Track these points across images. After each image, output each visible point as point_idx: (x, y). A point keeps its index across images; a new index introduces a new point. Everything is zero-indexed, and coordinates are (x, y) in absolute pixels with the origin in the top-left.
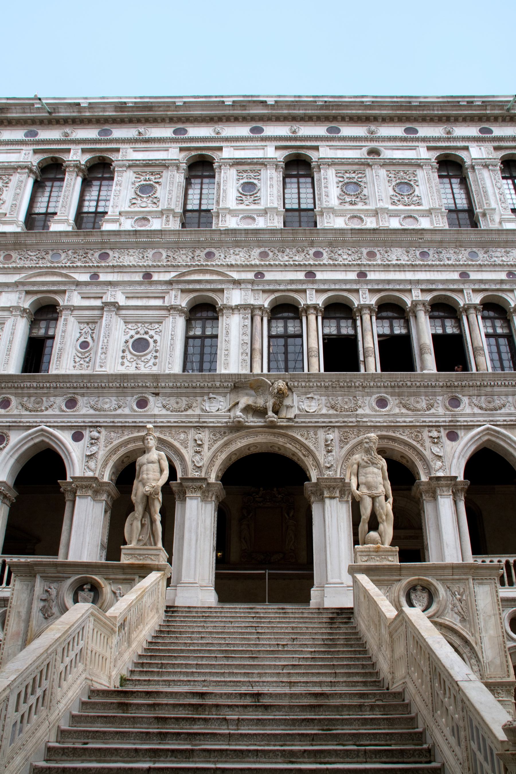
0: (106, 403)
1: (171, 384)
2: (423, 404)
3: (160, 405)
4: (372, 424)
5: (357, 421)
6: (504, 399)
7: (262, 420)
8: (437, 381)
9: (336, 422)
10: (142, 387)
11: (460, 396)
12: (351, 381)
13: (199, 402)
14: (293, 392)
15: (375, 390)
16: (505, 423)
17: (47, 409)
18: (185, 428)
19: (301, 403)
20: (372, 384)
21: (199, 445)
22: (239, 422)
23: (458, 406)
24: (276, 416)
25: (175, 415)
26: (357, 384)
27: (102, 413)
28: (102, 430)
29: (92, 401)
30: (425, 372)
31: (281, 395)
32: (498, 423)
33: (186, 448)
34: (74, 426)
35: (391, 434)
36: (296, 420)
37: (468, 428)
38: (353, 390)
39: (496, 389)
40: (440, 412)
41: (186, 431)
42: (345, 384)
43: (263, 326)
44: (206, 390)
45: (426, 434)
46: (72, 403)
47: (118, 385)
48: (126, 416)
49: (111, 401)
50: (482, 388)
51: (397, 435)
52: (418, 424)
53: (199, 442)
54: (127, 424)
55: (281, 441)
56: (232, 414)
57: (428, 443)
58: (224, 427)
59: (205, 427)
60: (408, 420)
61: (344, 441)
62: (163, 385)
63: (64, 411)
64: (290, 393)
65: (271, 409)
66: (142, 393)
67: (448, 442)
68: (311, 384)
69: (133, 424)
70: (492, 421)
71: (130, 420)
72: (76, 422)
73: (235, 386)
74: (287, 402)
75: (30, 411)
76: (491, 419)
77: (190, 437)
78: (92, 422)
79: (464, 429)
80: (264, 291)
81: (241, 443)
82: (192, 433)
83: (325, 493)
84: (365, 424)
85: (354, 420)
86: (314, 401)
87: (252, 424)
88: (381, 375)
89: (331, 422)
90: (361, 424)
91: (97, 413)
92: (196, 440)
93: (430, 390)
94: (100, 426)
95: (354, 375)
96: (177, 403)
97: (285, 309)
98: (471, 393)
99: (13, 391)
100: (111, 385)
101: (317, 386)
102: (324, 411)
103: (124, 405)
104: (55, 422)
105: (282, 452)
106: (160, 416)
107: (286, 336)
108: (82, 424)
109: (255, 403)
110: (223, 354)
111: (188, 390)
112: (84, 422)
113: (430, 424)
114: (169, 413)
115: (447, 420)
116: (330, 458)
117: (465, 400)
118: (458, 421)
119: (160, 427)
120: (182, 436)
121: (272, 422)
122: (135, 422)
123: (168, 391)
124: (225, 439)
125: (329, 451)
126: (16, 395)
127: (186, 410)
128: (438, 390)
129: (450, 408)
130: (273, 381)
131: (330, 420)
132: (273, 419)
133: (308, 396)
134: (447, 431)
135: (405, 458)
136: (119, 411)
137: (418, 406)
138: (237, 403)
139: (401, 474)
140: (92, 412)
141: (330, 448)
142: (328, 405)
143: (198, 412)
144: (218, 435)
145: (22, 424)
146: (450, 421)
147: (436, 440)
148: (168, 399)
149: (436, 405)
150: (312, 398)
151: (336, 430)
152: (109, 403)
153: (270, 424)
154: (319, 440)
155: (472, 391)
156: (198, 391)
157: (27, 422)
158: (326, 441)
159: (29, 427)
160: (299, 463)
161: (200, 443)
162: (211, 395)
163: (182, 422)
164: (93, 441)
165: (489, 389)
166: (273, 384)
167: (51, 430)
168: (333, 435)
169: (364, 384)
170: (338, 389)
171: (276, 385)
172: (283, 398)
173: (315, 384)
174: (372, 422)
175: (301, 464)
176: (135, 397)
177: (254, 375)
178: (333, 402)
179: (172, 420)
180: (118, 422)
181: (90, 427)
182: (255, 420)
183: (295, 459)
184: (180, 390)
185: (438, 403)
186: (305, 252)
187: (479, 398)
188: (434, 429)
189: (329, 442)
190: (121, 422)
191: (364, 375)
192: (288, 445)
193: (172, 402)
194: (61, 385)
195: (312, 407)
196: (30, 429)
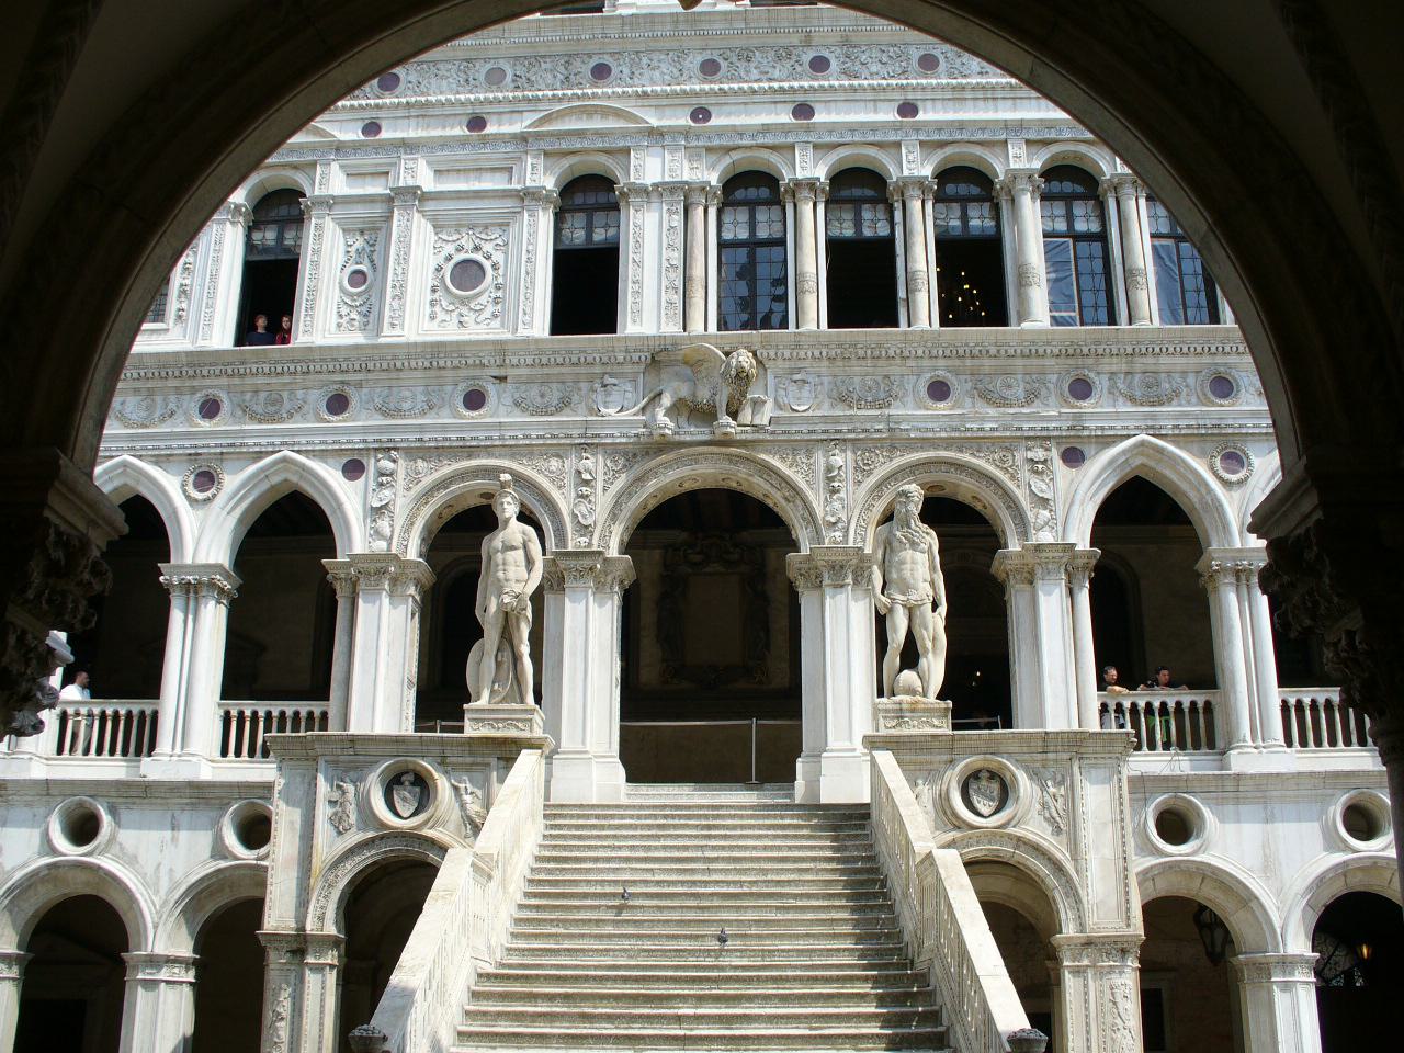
0: (405, 399)
3: (509, 401)
4: (919, 435)
5: (890, 430)
6: (1179, 380)
7: (706, 430)
8: (1048, 343)
10: (475, 366)
11: (1092, 375)
13: (584, 391)
14: (766, 370)
15: (926, 363)
16: (1177, 432)
17: (291, 416)
21: (587, 483)
24: (733, 423)
30: (1025, 325)
32: (1163, 432)
33: (560, 487)
34: (346, 450)
37: (1106, 441)
38: (880, 363)
39: (1164, 360)
41: (561, 453)
42: (869, 352)
43: (706, 227)
47: (427, 364)
49: (414, 397)
50: (1138, 359)
51: (966, 457)
53: (586, 476)
59: (597, 445)
60: (988, 426)
62: (515, 361)
65: (724, 408)
66: (474, 378)
68: (802, 354)
69: (461, 444)
70: (1152, 427)
73: (653, 358)
79: (1096, 443)
80: (709, 150)
84: (904, 435)
86: (807, 387)
87: (688, 438)
88: (939, 334)
89: (840, 431)
92: (580, 472)
93: (1035, 361)
94: (395, 449)
95: (887, 333)
96: (542, 396)
97: (751, 187)
98: (1114, 368)
99: (224, 381)
100: (413, 364)
102: (825, 411)
104: (308, 443)
107: (753, 244)
108: (361, 446)
109: (694, 395)
110: (630, 290)
113: (1032, 434)
117: (1101, 383)
118: (1084, 428)
120: (554, 463)
123: (524, 371)
125: (834, 491)
127: (559, 410)
130: (727, 348)
132: (729, 430)
134: (1063, 448)
135: (980, 501)
138: (660, 394)
141: (836, 484)
142: (835, 394)
146: (1069, 429)
147: (1040, 466)
148: (523, 387)
149: (1044, 392)
150: (804, 381)
153: (722, 438)
156: (583, 370)
160: (776, 510)
161: (588, 477)
162: (608, 380)
165: (1150, 360)
166: (727, 354)
169: (906, 353)
170: (854, 362)
172: (747, 385)
173: (810, 354)
174: (919, 430)
177: (690, 337)
178: (843, 389)
181: (376, 449)
184: (546, 370)
185: (1047, 388)
186: (794, 58)
187: (1130, 376)
191: (905, 333)
194: (318, 368)
196: (260, 458)
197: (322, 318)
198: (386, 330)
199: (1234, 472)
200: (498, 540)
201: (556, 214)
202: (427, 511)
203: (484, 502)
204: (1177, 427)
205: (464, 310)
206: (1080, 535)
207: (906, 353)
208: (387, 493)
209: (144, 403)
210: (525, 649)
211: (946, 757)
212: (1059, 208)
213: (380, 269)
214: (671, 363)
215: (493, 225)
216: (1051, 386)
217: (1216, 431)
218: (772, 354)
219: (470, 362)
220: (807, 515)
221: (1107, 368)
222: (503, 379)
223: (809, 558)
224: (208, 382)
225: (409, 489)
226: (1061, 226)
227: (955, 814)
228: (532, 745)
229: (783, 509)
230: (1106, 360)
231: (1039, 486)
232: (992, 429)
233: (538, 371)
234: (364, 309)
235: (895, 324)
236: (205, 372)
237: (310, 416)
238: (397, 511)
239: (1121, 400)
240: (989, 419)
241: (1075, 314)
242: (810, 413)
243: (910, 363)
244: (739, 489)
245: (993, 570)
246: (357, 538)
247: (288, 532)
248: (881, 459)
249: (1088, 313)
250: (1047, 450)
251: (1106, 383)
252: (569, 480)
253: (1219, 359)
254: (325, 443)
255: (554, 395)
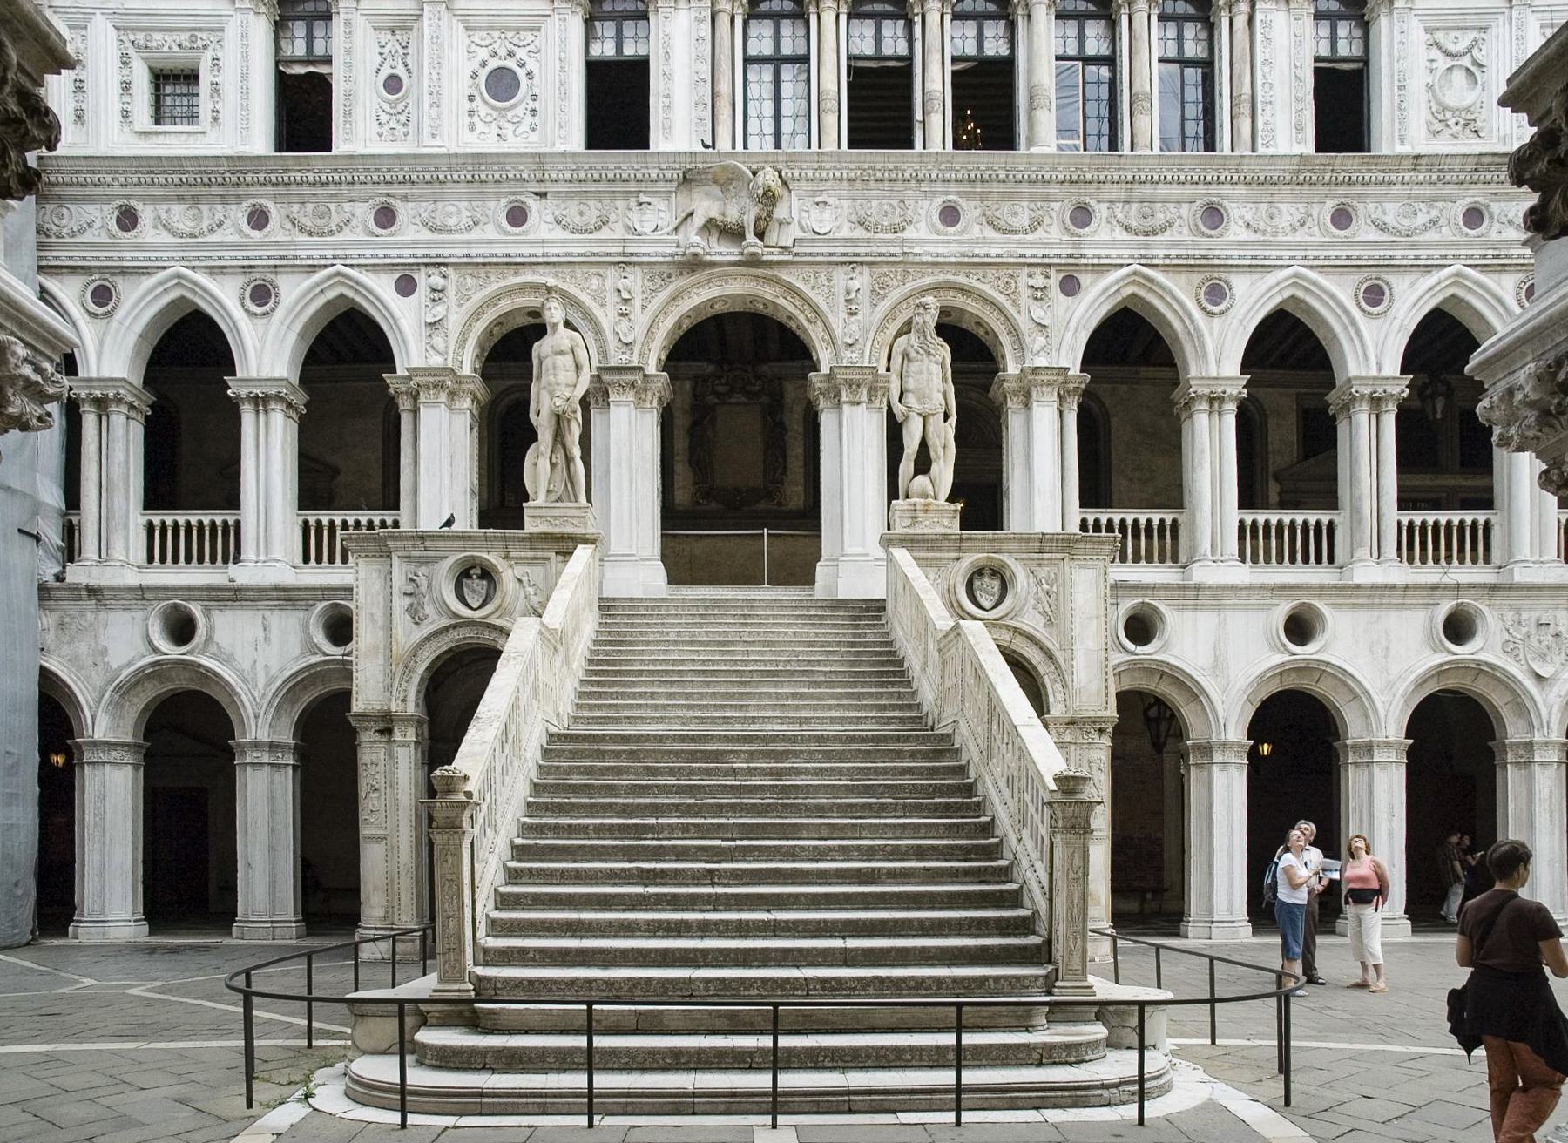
0: (450, 215)
1: (568, 176)
2: (1023, 220)
3: (550, 218)
4: (930, 259)
7: (736, 251)
9: (867, 254)
12: (897, 168)
15: (939, 187)
16: (1167, 261)
18: (597, 265)
19: (805, 214)
20: (934, 176)
22: (695, 255)
23: (1085, 224)
25: (579, 241)
26: (907, 176)
27: (445, 237)
28: (450, 271)
29: (425, 209)
31: (769, 199)
32: (1155, 261)
35: (961, 279)
36: (795, 250)
37: (1100, 268)
40: (1053, 238)
44: (633, 187)
45: (1023, 279)
46: (386, 217)
48: (490, 241)
50: (1136, 186)
52: (1012, 260)
54: (494, 260)
55: (768, 292)
56: (680, 237)
57: (1025, 293)
58: (668, 263)
59: (634, 264)
60: (993, 251)
61: (878, 293)
62: (554, 176)
63: (373, 234)
64: (786, 193)
66: (514, 193)
67: (1061, 296)
68: (824, 175)
70: (1145, 257)
71: (499, 251)
72: (399, 257)
74: (780, 212)
75: (310, 234)
76: (1143, 252)
77: (608, 283)
78: (428, 256)
81: (702, 295)
82: (612, 277)
83: (844, 394)
84: (917, 259)
85: (897, 250)
88: (953, 156)
89: (857, 255)
90: (911, 258)
91: (436, 236)
93: (1040, 188)
96: (581, 214)
98: (1114, 196)
101: (835, 179)
102: (845, 232)
103: (483, 219)
105: (769, 312)
106: (553, 241)
111: (601, 187)
112: (415, 256)
114: (567, 235)
115: (1064, 252)
116: (854, 327)
117: (1101, 211)
118: (1082, 256)
119: (554, 264)
120: (595, 282)
121: (753, 254)
122: (508, 255)
123: (562, 187)
124: (672, 287)
125: (852, 314)
126: (275, 199)
127: (598, 228)
128: (1054, 189)
129: (1072, 227)
130: (754, 167)
131: (857, 250)
133: (818, 199)
136: (475, 234)
137: (1015, 222)
139: (972, 353)
140: (426, 235)
142: (854, 218)
143: (619, 233)
144: (658, 280)
145: (298, 262)
149: (1047, 220)
151: (866, 269)
152: (456, 212)
154: (836, 290)
155: (1118, 192)
156: (619, 187)
157: (308, 258)
158: (848, 293)
159: (313, 268)
163: (594, 254)
164: (436, 295)
166: (754, 174)
167: (354, 273)
168: (861, 281)
169: (921, 176)
171: (760, 178)
172: (774, 205)
174: (930, 254)
175: (802, 336)
176: (504, 201)
179: (576, 251)
180: (478, 255)
181: (426, 265)
182: (723, 249)
183: (793, 325)
184: (584, 187)
188: (1039, 270)
189: (853, 296)
190: (483, 256)
191: (921, 155)
192: (781, 301)
193: (571, 210)
195: (822, 220)
197: (358, 127)
198: (428, 141)
199: (1216, 304)
200: (541, 348)
201: (586, 21)
202: (480, 327)
203: (532, 321)
204: (1167, 257)
205: (503, 123)
206: (1070, 356)
207: (921, 176)
208: (439, 311)
209: (191, 212)
210: (576, 452)
211: (954, 555)
212: (1072, 28)
213: (414, 74)
214: (702, 182)
215: (525, 29)
216: (1053, 214)
217: (1203, 262)
218: (796, 175)
219: (511, 176)
220: (827, 337)
221: (1106, 196)
222: (543, 195)
223: (830, 377)
224: (252, 190)
225: (460, 305)
226: (1072, 50)
227: (960, 606)
228: (585, 540)
229: (805, 331)
230: (1107, 187)
231: (1039, 313)
232: (998, 256)
233: (576, 187)
234: (403, 118)
235: (910, 145)
236: (248, 179)
237: (359, 230)
238: (450, 327)
239: (1118, 229)
240: (997, 246)
241: (1080, 142)
242: (831, 236)
243: (925, 187)
244: (765, 312)
245: (991, 394)
246: (413, 350)
247: (347, 350)
248: (895, 283)
249: (1092, 140)
250: (1047, 277)
251: (1105, 213)
252: (612, 298)
253: (1213, 189)
254: (376, 256)
255: (592, 217)
